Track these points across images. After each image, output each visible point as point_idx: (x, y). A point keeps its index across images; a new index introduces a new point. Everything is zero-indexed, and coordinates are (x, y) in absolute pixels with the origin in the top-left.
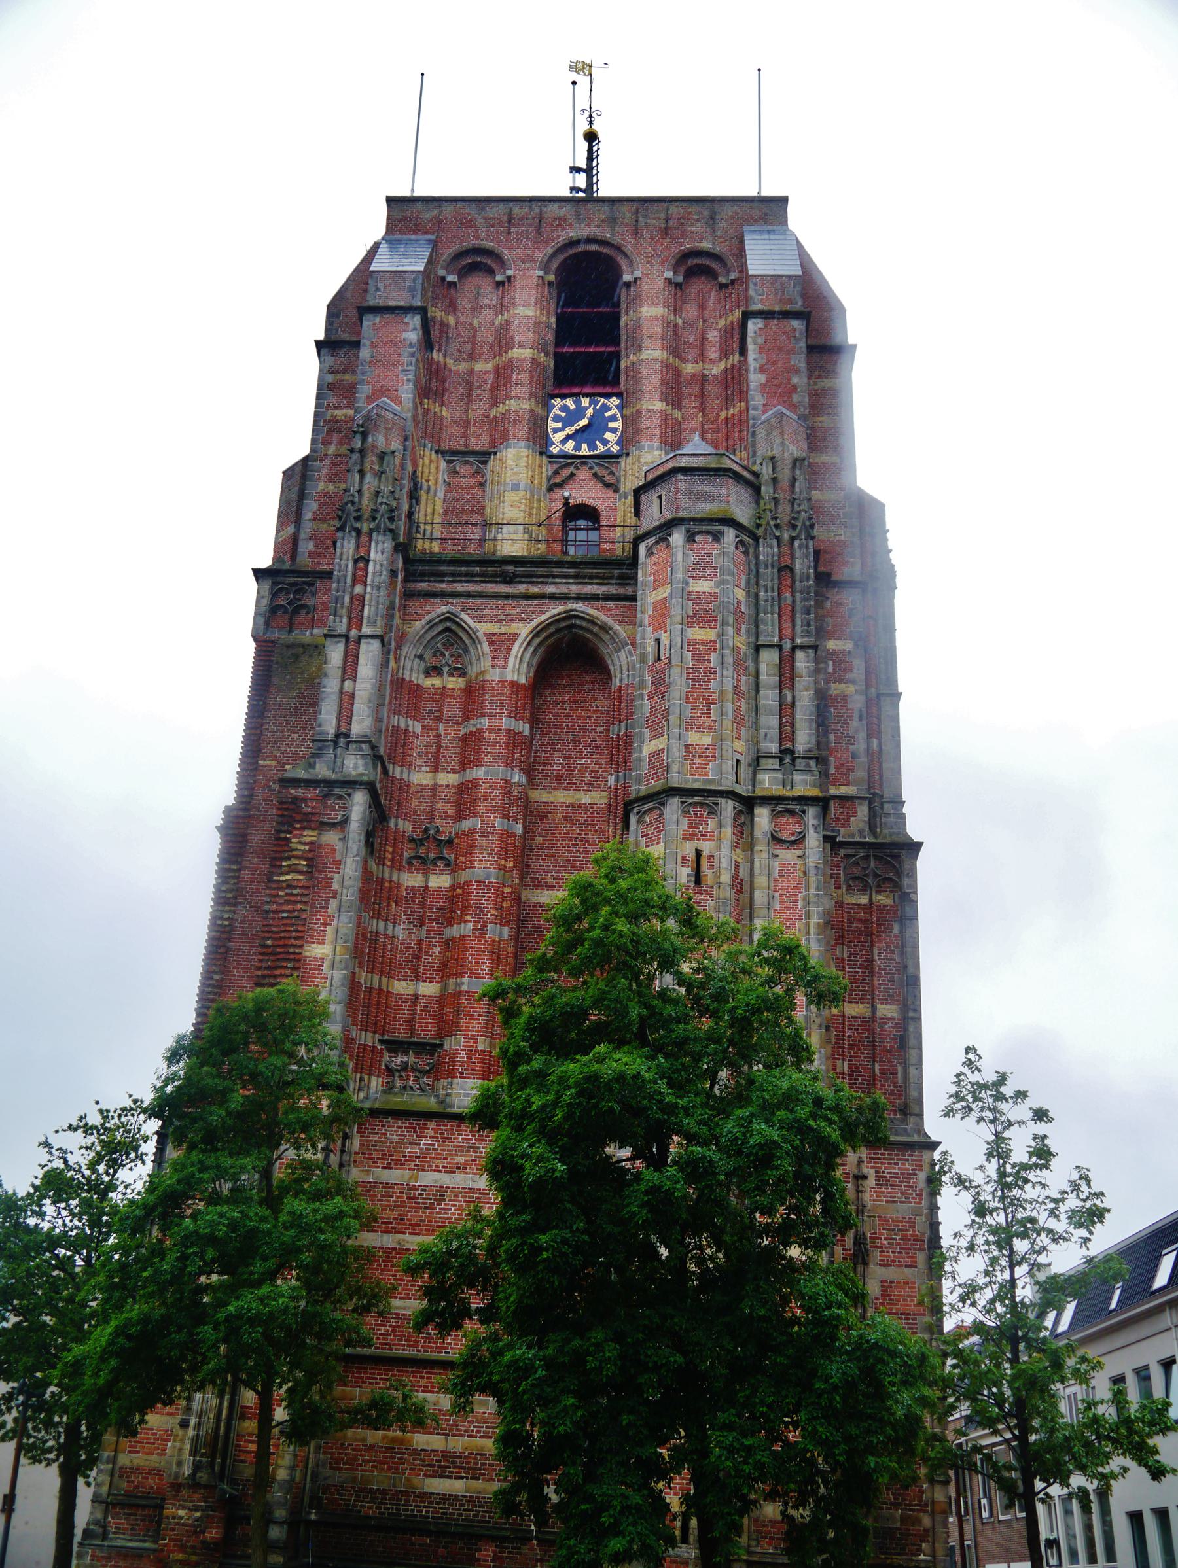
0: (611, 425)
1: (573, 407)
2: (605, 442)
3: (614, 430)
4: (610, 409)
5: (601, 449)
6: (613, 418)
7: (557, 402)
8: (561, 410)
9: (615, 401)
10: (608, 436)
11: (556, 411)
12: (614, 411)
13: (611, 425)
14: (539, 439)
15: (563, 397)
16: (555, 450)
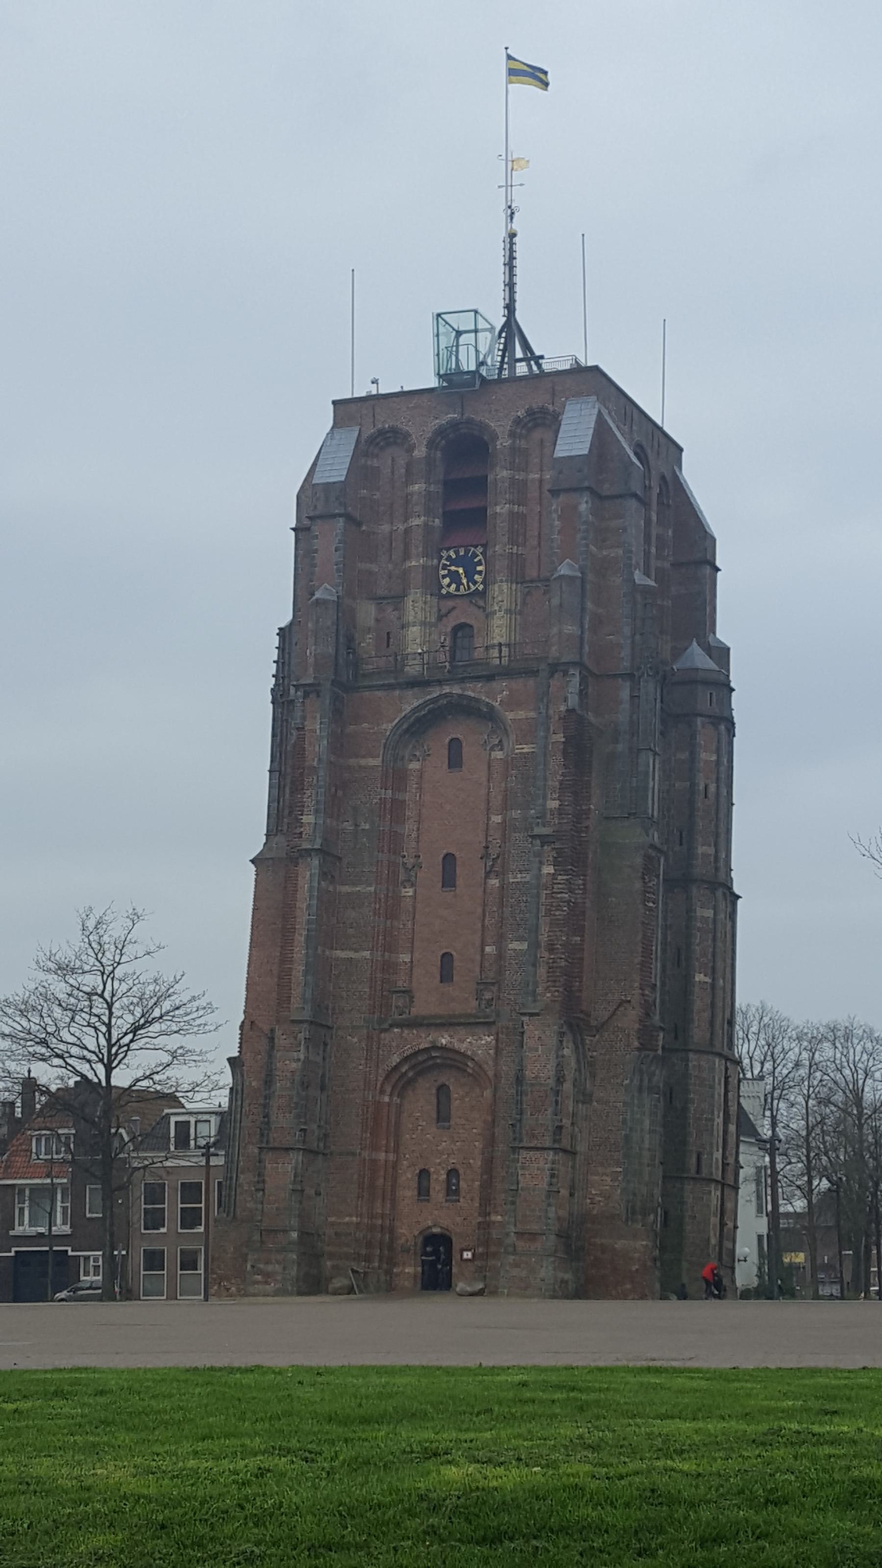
0: (479, 568)
1: (454, 557)
2: (475, 583)
3: (480, 573)
4: (478, 556)
5: (473, 588)
6: (479, 563)
7: (444, 554)
8: (447, 560)
9: (480, 550)
10: (477, 577)
11: (444, 561)
12: (481, 557)
13: (479, 568)
14: (433, 587)
15: (448, 549)
16: (444, 592)
